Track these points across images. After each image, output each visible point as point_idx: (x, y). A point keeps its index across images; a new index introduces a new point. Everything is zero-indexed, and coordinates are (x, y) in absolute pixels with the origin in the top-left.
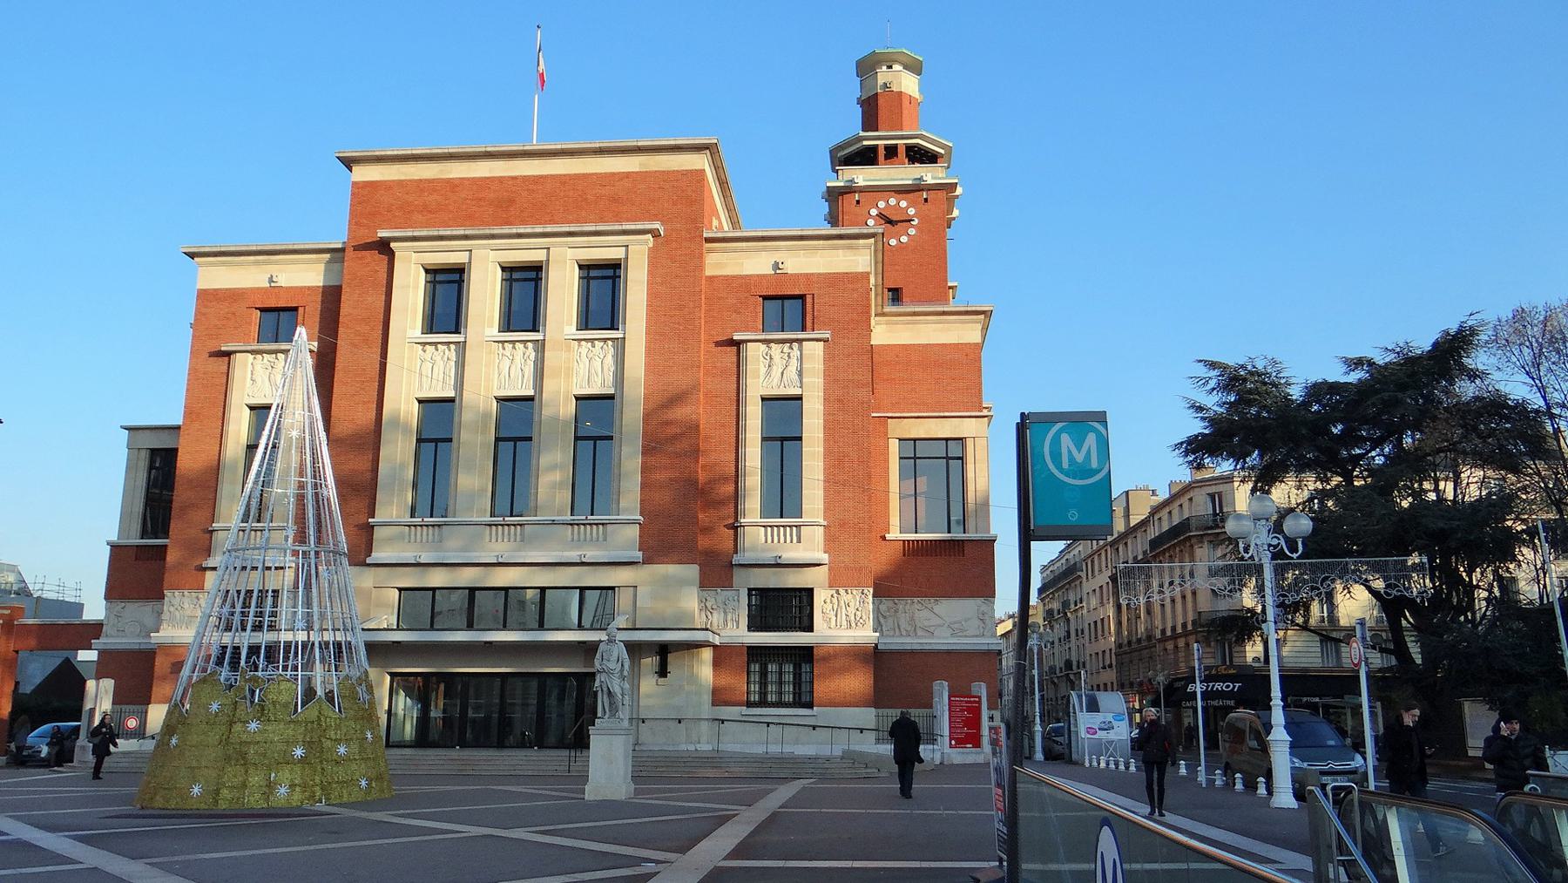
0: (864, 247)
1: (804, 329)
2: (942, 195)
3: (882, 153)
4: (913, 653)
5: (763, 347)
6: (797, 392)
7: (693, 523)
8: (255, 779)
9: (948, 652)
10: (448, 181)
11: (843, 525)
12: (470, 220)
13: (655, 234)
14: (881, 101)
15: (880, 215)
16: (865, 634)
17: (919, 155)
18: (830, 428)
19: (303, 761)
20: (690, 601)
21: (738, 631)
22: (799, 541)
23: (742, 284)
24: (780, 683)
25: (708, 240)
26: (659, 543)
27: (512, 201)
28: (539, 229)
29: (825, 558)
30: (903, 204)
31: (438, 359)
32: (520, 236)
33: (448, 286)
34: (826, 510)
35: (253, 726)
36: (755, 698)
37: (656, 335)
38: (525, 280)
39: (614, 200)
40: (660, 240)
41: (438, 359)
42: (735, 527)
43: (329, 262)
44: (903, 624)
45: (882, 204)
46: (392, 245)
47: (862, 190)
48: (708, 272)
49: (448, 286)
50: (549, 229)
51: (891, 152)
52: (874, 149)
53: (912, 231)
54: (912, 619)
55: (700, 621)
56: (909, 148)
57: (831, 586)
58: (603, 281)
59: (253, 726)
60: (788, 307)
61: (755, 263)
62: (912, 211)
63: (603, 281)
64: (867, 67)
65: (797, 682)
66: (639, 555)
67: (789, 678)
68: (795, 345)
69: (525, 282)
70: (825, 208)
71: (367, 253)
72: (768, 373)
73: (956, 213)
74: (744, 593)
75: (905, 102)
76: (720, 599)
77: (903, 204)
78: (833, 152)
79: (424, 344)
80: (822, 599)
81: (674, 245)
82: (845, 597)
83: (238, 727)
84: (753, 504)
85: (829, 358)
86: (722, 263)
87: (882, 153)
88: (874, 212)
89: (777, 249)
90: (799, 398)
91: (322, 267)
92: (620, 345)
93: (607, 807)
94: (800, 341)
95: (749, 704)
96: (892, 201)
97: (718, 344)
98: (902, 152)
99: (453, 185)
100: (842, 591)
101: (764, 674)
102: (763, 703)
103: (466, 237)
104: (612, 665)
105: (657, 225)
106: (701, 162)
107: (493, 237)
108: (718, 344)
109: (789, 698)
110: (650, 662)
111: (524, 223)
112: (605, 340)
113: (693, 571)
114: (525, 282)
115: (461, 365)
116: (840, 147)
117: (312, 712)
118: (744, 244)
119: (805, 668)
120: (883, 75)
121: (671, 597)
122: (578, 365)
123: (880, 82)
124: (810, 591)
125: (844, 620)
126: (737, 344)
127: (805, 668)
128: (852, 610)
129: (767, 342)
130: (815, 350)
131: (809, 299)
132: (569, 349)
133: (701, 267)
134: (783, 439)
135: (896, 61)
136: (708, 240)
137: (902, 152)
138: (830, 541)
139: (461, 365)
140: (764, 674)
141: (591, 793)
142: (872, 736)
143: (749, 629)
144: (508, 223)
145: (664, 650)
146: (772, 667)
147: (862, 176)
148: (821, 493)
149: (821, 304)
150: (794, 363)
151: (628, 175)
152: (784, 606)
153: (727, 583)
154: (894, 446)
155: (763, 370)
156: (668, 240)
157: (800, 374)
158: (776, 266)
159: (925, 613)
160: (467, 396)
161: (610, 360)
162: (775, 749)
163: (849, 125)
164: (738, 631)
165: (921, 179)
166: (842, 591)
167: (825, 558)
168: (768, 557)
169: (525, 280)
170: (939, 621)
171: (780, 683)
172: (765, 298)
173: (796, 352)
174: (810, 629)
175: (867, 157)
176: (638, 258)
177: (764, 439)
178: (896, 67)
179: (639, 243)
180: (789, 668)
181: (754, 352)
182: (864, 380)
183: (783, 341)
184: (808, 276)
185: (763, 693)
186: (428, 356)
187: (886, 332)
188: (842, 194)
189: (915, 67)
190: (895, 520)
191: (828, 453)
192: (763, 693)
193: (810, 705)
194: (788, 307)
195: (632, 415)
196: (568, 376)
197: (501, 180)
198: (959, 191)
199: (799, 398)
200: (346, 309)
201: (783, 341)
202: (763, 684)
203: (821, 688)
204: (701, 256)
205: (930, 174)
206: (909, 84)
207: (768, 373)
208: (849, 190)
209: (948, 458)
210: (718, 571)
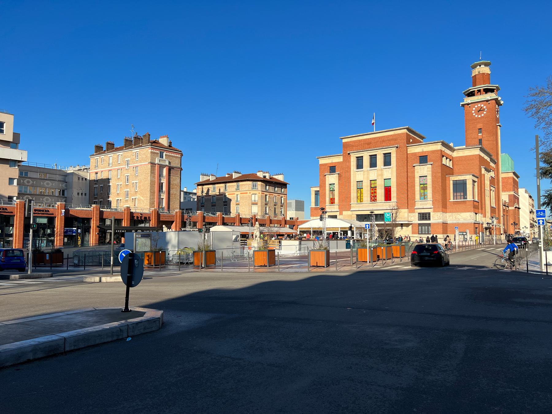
9: (463, 223)
23: (414, 154)
27: (370, 143)
29: (432, 207)
33: (360, 160)
49: (360, 160)
53: (485, 113)
56: (484, 90)
58: (387, 157)
62: (485, 107)
63: (387, 157)
74: (417, 215)
77: (482, 105)
98: (482, 91)
99: (360, 141)
137: (482, 91)
146: (423, 227)
153: (413, 212)
154: (451, 182)
159: (458, 216)
164: (417, 222)
167: (432, 207)
174: (429, 219)
180: (426, 227)
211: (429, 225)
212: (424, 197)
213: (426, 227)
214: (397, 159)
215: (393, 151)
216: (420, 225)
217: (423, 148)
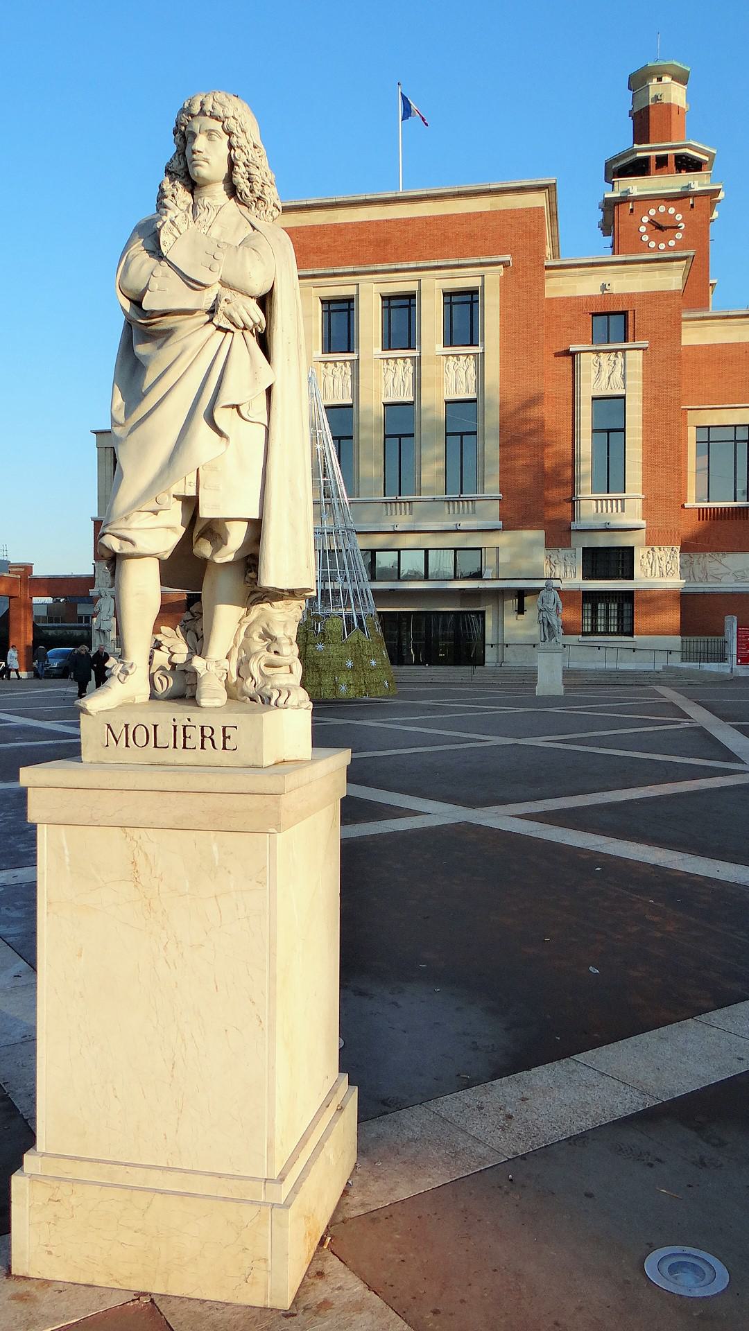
0: (679, 268)
1: (626, 340)
2: (706, 200)
3: (653, 163)
4: (704, 594)
5: (593, 356)
6: (621, 392)
7: (539, 499)
8: (327, 680)
9: (733, 594)
10: (335, 226)
11: (657, 497)
12: (355, 258)
13: (505, 265)
14: (652, 113)
15: (651, 222)
16: (675, 582)
17: (688, 164)
18: (647, 421)
19: (352, 669)
20: (540, 557)
21: (574, 580)
22: (623, 511)
24: (607, 618)
25: (548, 268)
26: (518, 514)
28: (413, 265)
29: (643, 523)
30: (672, 211)
31: (337, 374)
32: (397, 271)
34: (645, 486)
35: (320, 646)
36: (588, 629)
37: (508, 349)
38: (401, 307)
39: (470, 236)
40: (509, 269)
41: (337, 374)
42: (572, 501)
44: (697, 573)
45: (652, 212)
47: (636, 199)
48: (547, 295)
50: (421, 264)
51: (662, 162)
52: (646, 160)
53: (679, 236)
54: (704, 568)
55: (546, 572)
56: (678, 157)
57: (647, 545)
59: (320, 646)
60: (613, 321)
61: (586, 286)
63: (464, 303)
64: (638, 81)
65: (620, 618)
67: (614, 614)
68: (620, 354)
69: (401, 307)
70: (600, 215)
72: (598, 378)
73: (715, 215)
75: (674, 112)
76: (561, 557)
77: (672, 211)
78: (608, 165)
79: (326, 362)
80: (639, 554)
81: (520, 273)
82: (658, 553)
83: (310, 647)
84: (585, 484)
85: (647, 363)
86: (559, 286)
87: (653, 163)
88: (645, 219)
89: (604, 273)
90: (624, 397)
92: (480, 359)
93: (552, 700)
94: (624, 350)
95: (584, 634)
96: (662, 209)
97: (557, 355)
98: (671, 161)
99: (339, 229)
100: (656, 549)
101: (594, 611)
102: (594, 632)
103: (354, 274)
104: (550, 606)
105: (508, 258)
106: (539, 200)
107: (376, 272)
108: (557, 355)
109: (613, 629)
110: (511, 604)
111: (399, 259)
112: (468, 355)
113: (539, 535)
114: (401, 307)
115: (356, 377)
116: (616, 160)
117: (353, 638)
118: (577, 270)
119: (627, 607)
120: (654, 88)
121: (519, 554)
122: (449, 376)
123: (652, 95)
124: (630, 551)
125: (658, 570)
126: (573, 354)
127: (627, 607)
128: (663, 563)
129: (597, 352)
130: (636, 357)
131: (630, 315)
132: (440, 363)
133: (542, 291)
134: (609, 431)
135: (666, 73)
136: (548, 268)
137: (671, 161)
138: (647, 509)
139: (356, 377)
140: (594, 611)
141: (540, 690)
142: (678, 656)
143: (583, 578)
144: (385, 260)
145: (521, 594)
146: (601, 607)
147: (636, 186)
148: (641, 473)
149: (640, 320)
150: (619, 368)
151: (481, 214)
152: (611, 560)
153: (566, 544)
154: (692, 433)
155: (594, 375)
156: (515, 270)
157: (624, 378)
158: (604, 287)
159: (715, 565)
160: (364, 402)
161: (472, 371)
162: (611, 666)
163: (621, 140)
164: (574, 580)
165: (688, 186)
166: (656, 549)
167: (643, 523)
168: (598, 524)
169: (401, 307)
170: (726, 570)
171: (607, 618)
172: (594, 315)
173: (620, 360)
174: (632, 578)
175: (639, 168)
176: (491, 283)
177: (593, 431)
178: (667, 79)
179: (493, 273)
180: (613, 606)
181: (587, 360)
182: (673, 378)
183: (610, 351)
184: (629, 296)
185: (594, 626)
186: (329, 371)
187: (692, 336)
188: (618, 204)
189: (682, 78)
190: (691, 493)
191: (646, 441)
192: (594, 626)
193: (631, 634)
194: (613, 321)
195: (492, 419)
196: (440, 384)
197: (378, 223)
198: (722, 195)
199: (624, 397)
201: (610, 351)
202: (594, 617)
203: (639, 623)
204: (543, 284)
205: (696, 182)
206: (676, 94)
207: (598, 378)
208: (624, 200)
209: (736, 441)
210: (559, 534)
211: (628, 596)
212: (611, 477)
213: (613, 606)
214: (504, 316)
215: (491, 283)
216: (590, 597)
217: (605, 279)
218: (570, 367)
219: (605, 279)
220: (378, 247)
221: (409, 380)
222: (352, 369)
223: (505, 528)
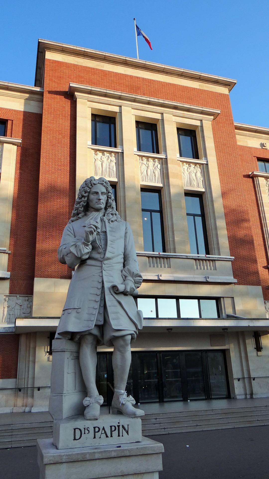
32: (149, 103)
43: (26, 99)
46: (76, 93)
61: (253, 142)
63: (189, 134)
66: (231, 279)
71: (58, 97)
91: (23, 101)
110: (250, 344)
113: (259, 289)
126: (253, 177)
158: (262, 145)
161: (199, 174)
172: (259, 159)
195: (218, 205)
197: (131, 77)
200: (44, 124)
218: (252, 184)
219: (263, 141)
220: (134, 90)
221: (158, 172)
222: (117, 159)
223: (238, 283)
